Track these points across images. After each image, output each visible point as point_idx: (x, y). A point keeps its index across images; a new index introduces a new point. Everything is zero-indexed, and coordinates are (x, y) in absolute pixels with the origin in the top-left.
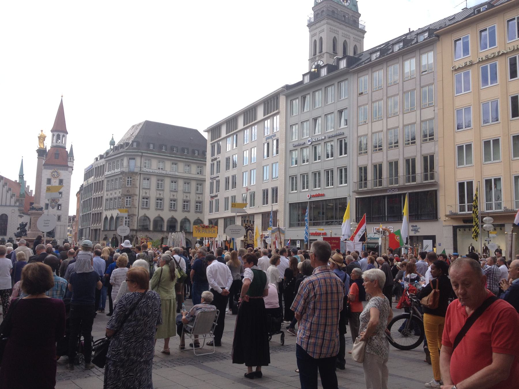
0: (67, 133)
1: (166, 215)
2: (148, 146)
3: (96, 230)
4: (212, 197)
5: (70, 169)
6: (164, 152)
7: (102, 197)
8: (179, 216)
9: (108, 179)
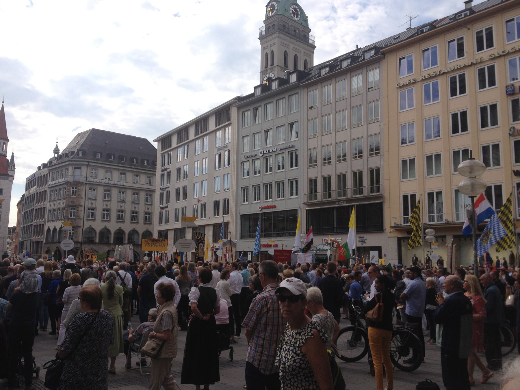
0: (8, 141)
1: (113, 227)
2: (95, 154)
3: (38, 243)
4: (162, 208)
5: (10, 178)
6: (111, 162)
7: (44, 208)
8: (127, 227)
9: (51, 189)
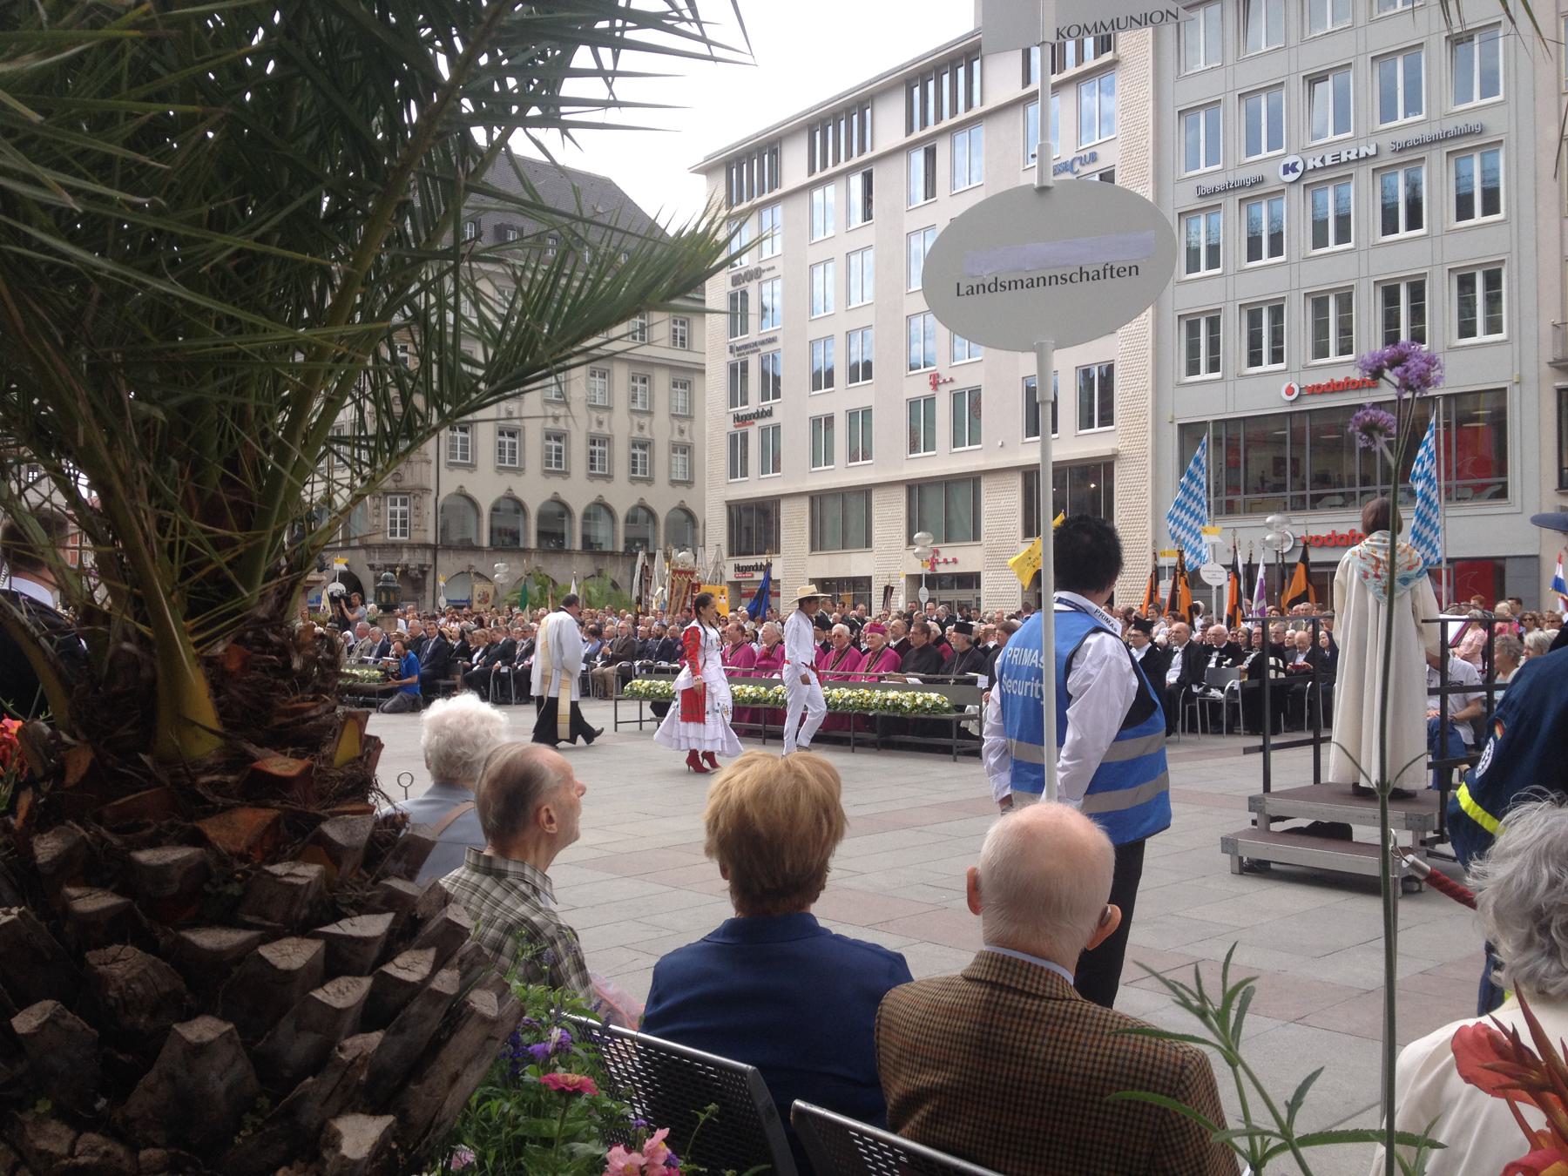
1: (534, 491)
4: (741, 420)
8: (578, 493)
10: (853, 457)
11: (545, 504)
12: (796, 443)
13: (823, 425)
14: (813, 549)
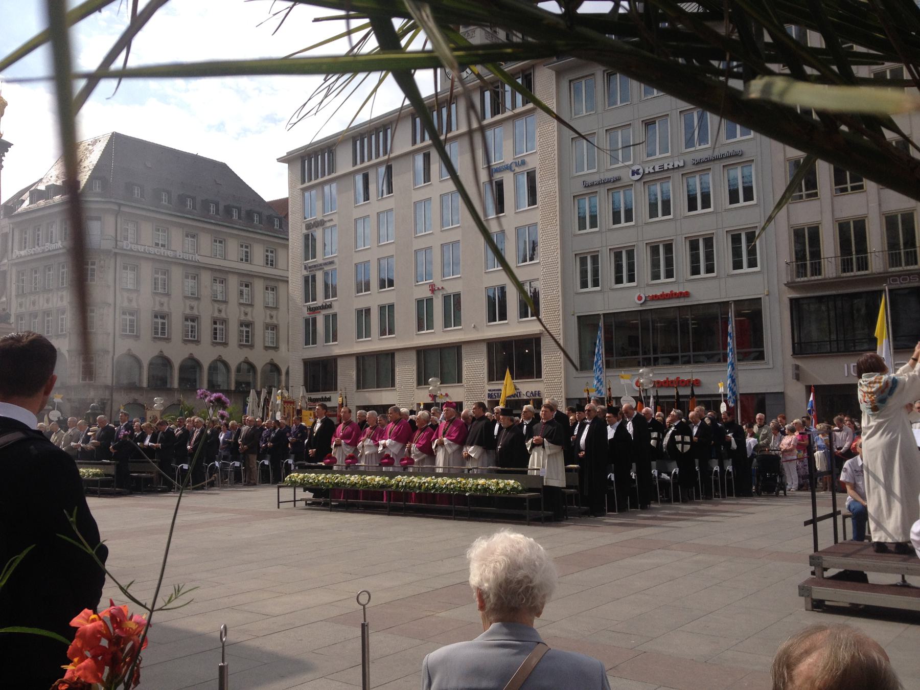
4: (312, 310)
8: (206, 354)
10: (383, 333)
11: (184, 361)
12: (347, 324)
13: (364, 314)
14: (358, 388)
